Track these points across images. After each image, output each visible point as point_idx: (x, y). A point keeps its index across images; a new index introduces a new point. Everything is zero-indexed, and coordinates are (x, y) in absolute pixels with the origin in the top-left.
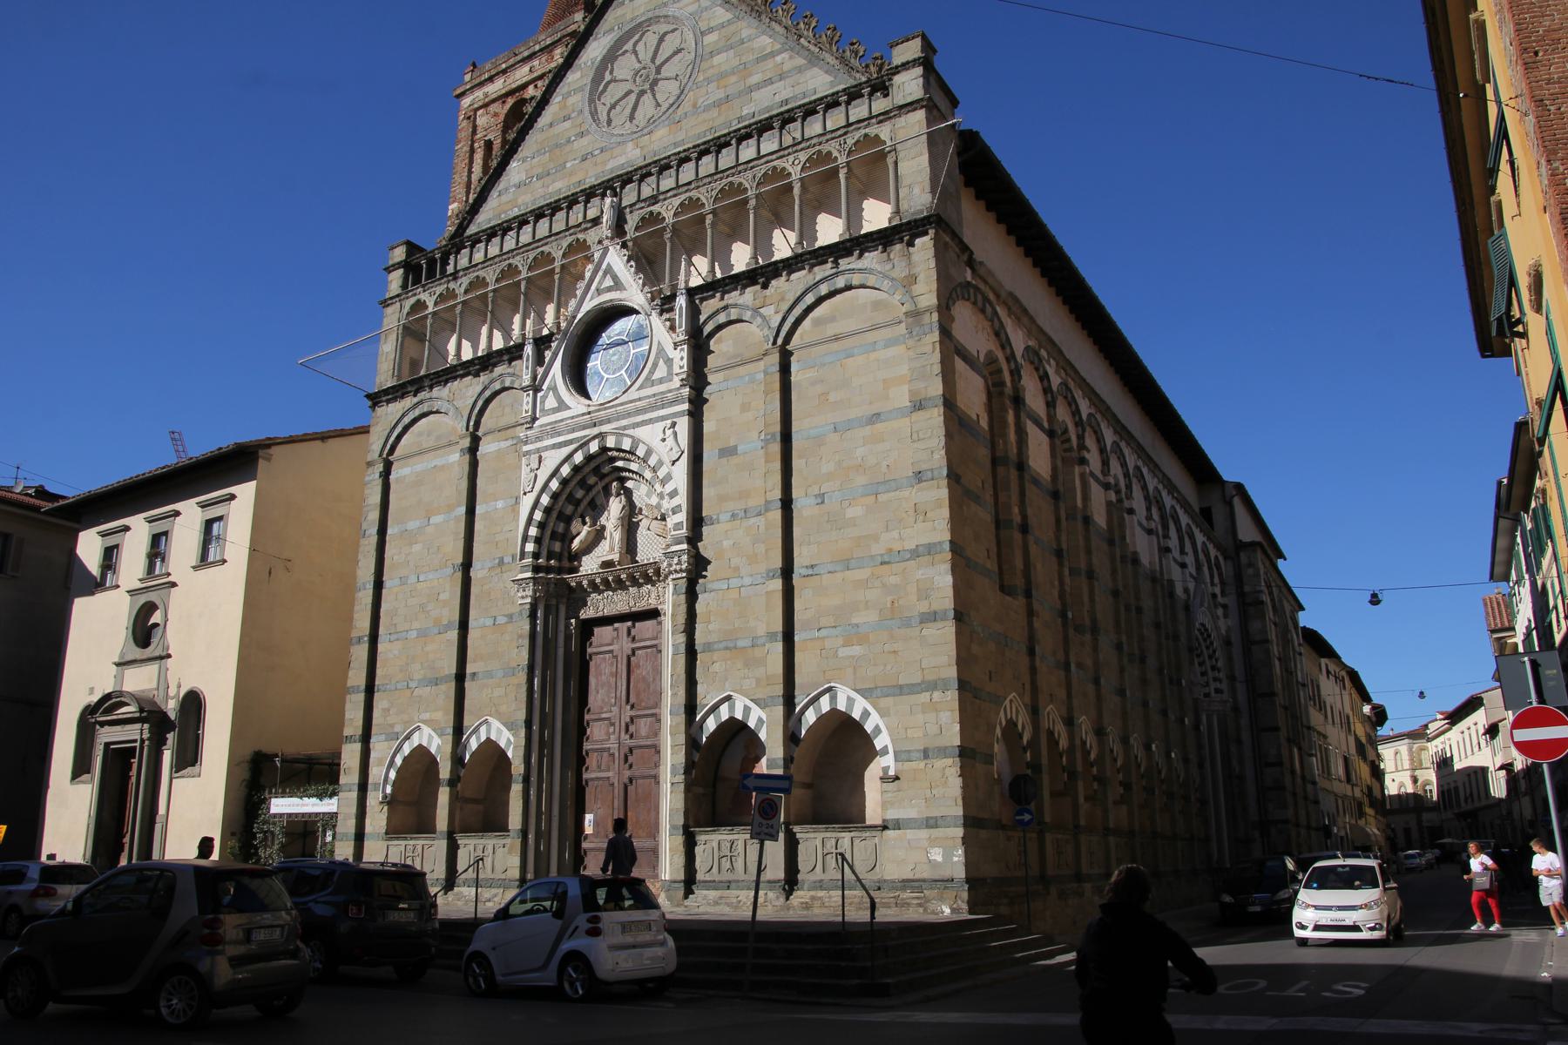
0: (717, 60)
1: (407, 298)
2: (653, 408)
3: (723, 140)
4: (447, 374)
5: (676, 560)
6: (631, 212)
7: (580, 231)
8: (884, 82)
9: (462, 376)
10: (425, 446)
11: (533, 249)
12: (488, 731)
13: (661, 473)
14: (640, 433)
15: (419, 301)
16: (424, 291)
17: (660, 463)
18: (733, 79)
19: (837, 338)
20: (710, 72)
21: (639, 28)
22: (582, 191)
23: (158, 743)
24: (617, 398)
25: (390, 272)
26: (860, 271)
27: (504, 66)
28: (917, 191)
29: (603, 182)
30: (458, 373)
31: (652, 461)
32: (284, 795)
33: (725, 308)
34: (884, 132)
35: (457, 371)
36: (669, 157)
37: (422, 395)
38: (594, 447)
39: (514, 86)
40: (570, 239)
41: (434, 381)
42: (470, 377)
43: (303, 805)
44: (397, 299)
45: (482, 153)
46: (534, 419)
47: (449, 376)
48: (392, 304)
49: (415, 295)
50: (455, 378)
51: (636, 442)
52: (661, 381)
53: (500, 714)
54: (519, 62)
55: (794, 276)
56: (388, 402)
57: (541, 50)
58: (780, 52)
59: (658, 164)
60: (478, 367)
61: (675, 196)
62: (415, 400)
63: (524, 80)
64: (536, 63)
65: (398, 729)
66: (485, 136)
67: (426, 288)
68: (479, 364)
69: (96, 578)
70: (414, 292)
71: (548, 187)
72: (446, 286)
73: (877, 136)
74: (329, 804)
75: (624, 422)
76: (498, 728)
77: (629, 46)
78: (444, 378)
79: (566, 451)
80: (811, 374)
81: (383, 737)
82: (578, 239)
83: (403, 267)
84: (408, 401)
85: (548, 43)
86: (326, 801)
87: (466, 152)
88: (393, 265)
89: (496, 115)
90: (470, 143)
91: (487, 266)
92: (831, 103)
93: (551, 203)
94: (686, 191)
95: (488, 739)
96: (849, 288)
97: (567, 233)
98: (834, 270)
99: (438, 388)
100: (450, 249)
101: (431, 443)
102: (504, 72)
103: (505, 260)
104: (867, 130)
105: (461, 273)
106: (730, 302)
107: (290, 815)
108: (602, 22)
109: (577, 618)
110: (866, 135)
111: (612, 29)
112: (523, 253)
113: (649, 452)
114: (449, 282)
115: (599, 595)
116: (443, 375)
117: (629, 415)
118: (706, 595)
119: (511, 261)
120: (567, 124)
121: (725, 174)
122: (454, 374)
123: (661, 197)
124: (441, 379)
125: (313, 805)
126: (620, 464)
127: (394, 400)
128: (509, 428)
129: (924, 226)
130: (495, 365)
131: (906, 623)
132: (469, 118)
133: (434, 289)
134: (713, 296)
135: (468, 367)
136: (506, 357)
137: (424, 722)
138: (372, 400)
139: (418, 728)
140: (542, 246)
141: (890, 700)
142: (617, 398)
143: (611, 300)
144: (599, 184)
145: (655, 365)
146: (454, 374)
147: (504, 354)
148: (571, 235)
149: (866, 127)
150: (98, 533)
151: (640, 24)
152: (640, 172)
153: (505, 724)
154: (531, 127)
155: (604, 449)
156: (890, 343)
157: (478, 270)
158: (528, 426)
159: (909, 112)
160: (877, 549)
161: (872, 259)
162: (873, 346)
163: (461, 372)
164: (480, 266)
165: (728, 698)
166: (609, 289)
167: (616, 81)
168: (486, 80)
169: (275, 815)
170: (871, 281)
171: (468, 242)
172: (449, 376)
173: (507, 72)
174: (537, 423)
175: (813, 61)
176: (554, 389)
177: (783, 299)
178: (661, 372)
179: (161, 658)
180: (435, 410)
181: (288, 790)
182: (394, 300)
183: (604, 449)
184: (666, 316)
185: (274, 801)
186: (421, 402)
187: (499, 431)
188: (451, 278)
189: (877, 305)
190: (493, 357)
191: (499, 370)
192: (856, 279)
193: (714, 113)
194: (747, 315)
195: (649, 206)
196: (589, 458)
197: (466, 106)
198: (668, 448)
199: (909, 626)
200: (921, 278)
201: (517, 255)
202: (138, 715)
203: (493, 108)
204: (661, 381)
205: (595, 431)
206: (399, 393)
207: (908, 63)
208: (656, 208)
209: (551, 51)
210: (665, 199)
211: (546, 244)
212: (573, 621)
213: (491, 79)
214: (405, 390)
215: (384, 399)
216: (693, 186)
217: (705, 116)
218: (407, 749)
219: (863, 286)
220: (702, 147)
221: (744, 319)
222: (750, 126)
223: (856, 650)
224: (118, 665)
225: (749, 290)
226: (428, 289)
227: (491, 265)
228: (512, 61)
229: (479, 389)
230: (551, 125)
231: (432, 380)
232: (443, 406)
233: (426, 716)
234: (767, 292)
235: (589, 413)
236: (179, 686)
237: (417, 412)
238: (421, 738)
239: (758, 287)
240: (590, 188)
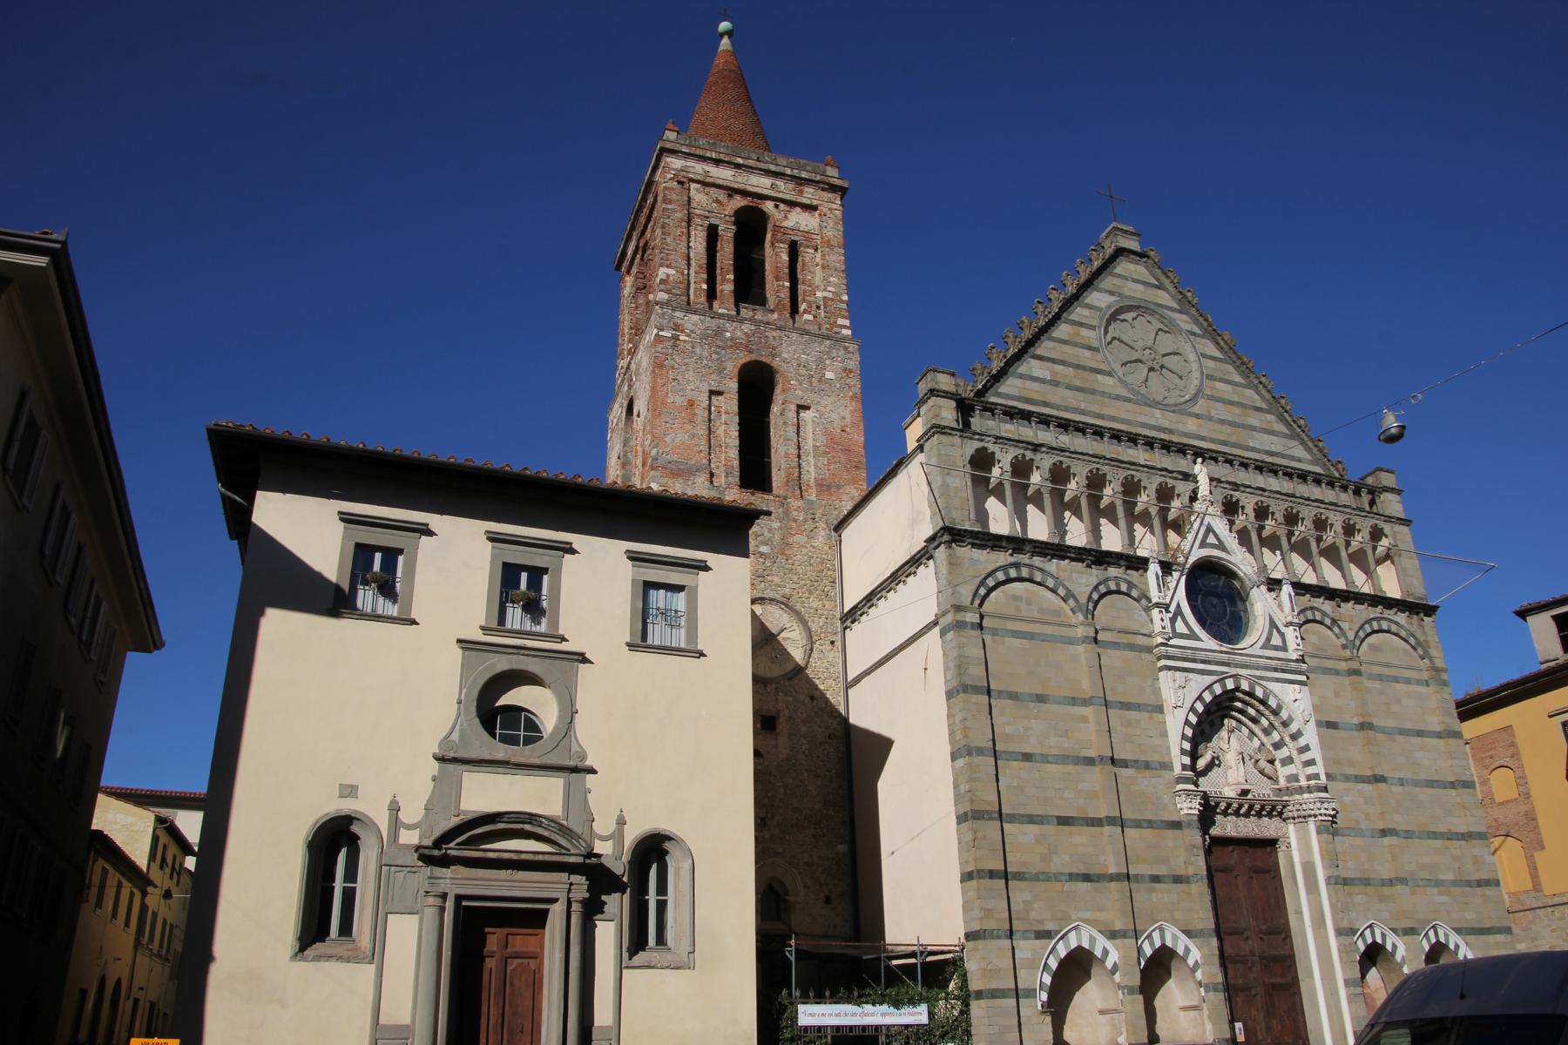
0: (1219, 385)
1: (971, 439)
2: (1276, 670)
3: (1275, 467)
4: (1057, 550)
5: (1326, 805)
6: (1216, 486)
7: (1171, 478)
8: (1375, 491)
9: (1072, 559)
10: (1024, 613)
11: (1124, 468)
12: (1162, 937)
13: (1293, 728)
14: (1274, 687)
15: (985, 449)
16: (995, 443)
17: (1291, 719)
18: (1237, 410)
19: (1388, 665)
20: (1215, 393)
21: (1139, 308)
22: (1161, 440)
23: (592, 909)
24: (1245, 649)
25: (938, 396)
26: (1397, 623)
27: (740, 161)
28: (1416, 582)
29: (1180, 444)
30: (1068, 555)
31: (1284, 715)
32: (820, 999)
33: (1312, 608)
34: (1387, 528)
35: (1070, 552)
36: (1236, 456)
37: (1017, 558)
38: (1230, 685)
39: (750, 189)
40: (1162, 479)
41: (1037, 550)
42: (1080, 564)
43: (867, 1015)
44: (958, 433)
45: (705, 233)
46: (1170, 638)
47: (1058, 553)
48: (950, 434)
49: (982, 440)
50: (1063, 558)
51: (1267, 693)
52: (1276, 648)
53: (1176, 920)
54: (760, 170)
55: (1357, 607)
56: (974, 546)
57: (792, 177)
58: (1268, 412)
59: (1226, 456)
60: (1093, 558)
61: (1251, 493)
62: (1012, 560)
63: (765, 192)
64: (780, 183)
65: (1050, 926)
66: (708, 217)
67: (998, 441)
68: (1094, 556)
69: (337, 588)
70: (984, 437)
71: (1080, 401)
72: (1022, 452)
73: (1382, 529)
74: (913, 1014)
75: (1258, 673)
76: (1173, 935)
77: (1129, 316)
78: (1051, 552)
79: (1209, 679)
80: (1376, 685)
81: (1033, 935)
82: (1166, 483)
83: (956, 400)
84: (1003, 558)
85: (803, 176)
86: (906, 1010)
87: (682, 220)
88: (944, 392)
89: (718, 201)
90: (686, 212)
91: (1074, 458)
92: (1303, 476)
93: (1131, 433)
94: (1260, 495)
95: (1164, 946)
96: (1388, 631)
97: (1159, 473)
98: (1380, 615)
99: (1042, 559)
100: (1016, 413)
101: (1036, 615)
102: (738, 166)
103: (1094, 462)
104: (1377, 522)
105: (1044, 449)
106: (1315, 605)
107: (838, 1028)
108: (1100, 278)
109: (1209, 834)
110: (1376, 525)
111: (1112, 293)
112: (1113, 466)
113: (1280, 707)
114: (1027, 449)
115: (1225, 817)
116: (1049, 549)
117: (1257, 668)
118: (1340, 838)
119: (1098, 466)
120: (1088, 353)
121: (1290, 499)
122: (1063, 554)
123: (1242, 488)
124: (1047, 551)
125: (884, 1015)
126: (1238, 704)
127: (981, 547)
128: (1130, 633)
129: (1431, 610)
130: (1109, 564)
131: (1469, 883)
132: (680, 183)
133: (1006, 447)
134: (1303, 595)
135: (1082, 554)
136: (1122, 563)
137: (1084, 921)
138: (950, 534)
139: (1076, 928)
140: (1133, 470)
141: (1472, 937)
142: (1245, 649)
143: (1220, 558)
144: (1176, 443)
145: (1270, 634)
146: (1063, 554)
147: (1122, 559)
148: (1161, 475)
149: (1377, 519)
150: (340, 513)
151: (1138, 307)
152: (1210, 453)
153: (1184, 932)
154: (1047, 332)
155: (1237, 689)
156: (1419, 682)
157: (1063, 456)
158: (1165, 641)
159: (1403, 524)
160: (1442, 828)
161: (1401, 618)
162: (1408, 681)
163: (1072, 555)
164: (1067, 454)
165: (1370, 926)
166: (1212, 546)
167: (1122, 341)
168: (711, 159)
169: (806, 1028)
170: (1403, 634)
171: (1036, 417)
172: (1058, 553)
173: (741, 169)
174: (1172, 642)
175: (1293, 436)
176: (1179, 611)
177: (1352, 621)
178: (1276, 640)
179: (575, 770)
180: (1039, 579)
181: (827, 993)
182: (955, 433)
183: (1237, 689)
184: (1274, 594)
185: (801, 1008)
186: (1017, 565)
187: (1119, 632)
188: (1030, 447)
189: (1404, 650)
190: (1111, 557)
191: (1113, 571)
192: (1394, 628)
193: (1227, 429)
194: (1328, 622)
195: (1231, 490)
196: (1226, 692)
197: (676, 167)
198: (1301, 710)
199: (1470, 886)
200: (1432, 645)
201: (1107, 464)
202: (580, 860)
203: (715, 193)
204: (1276, 648)
205: (1233, 671)
206: (989, 543)
207: (1393, 489)
208: (1236, 494)
209: (801, 185)
210: (1243, 492)
211: (1138, 471)
212: (1207, 837)
213: (717, 162)
214: (997, 543)
215: (970, 540)
216: (1266, 494)
217: (1218, 427)
218: (1062, 951)
219: (1396, 635)
220: (1260, 464)
221: (1325, 622)
222: (1295, 469)
223: (1445, 899)
224: (441, 759)
225: (1326, 602)
226: (1000, 443)
227: (1079, 459)
228: (751, 163)
229: (1094, 581)
230: (1065, 342)
231: (1035, 547)
232: (1050, 583)
233: (1087, 915)
234: (1340, 610)
235: (1221, 652)
236: (621, 822)
237: (1013, 573)
238: (1079, 938)
239: (1333, 603)
240: (1169, 442)
